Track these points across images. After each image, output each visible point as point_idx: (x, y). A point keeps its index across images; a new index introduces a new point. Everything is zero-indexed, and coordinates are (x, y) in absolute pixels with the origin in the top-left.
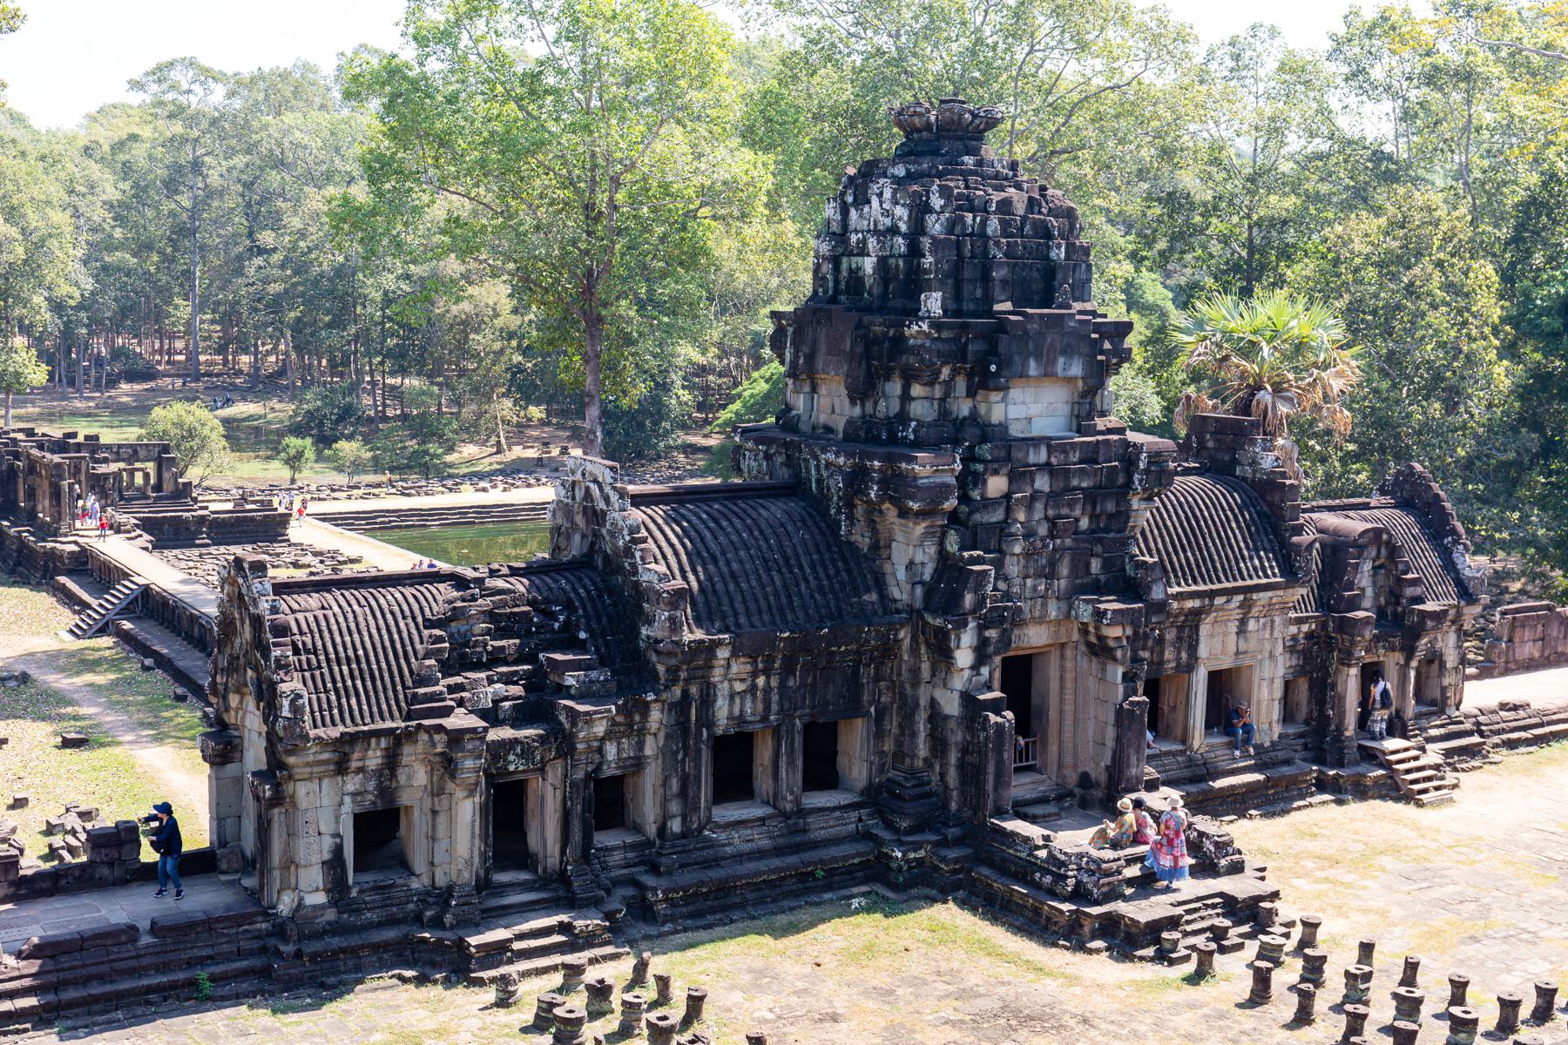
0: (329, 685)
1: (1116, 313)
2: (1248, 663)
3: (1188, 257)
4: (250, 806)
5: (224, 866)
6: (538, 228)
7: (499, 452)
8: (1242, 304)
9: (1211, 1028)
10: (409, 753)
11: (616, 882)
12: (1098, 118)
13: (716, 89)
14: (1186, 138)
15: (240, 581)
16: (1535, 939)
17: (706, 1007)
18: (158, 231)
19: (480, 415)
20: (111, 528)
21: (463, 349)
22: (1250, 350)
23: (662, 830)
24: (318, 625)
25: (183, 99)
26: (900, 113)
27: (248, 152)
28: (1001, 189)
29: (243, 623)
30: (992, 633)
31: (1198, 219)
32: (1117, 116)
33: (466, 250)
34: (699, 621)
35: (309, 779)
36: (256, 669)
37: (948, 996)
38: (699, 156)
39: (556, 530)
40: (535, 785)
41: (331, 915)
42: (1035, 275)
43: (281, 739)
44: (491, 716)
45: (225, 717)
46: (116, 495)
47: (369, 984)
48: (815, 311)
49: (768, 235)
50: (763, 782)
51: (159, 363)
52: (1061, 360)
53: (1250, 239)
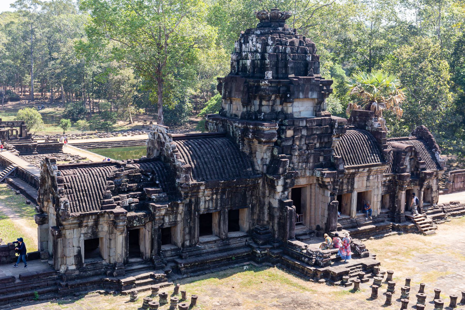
0: (76, 199)
1: (328, 77)
2: (370, 190)
3: (350, 60)
4: (51, 238)
5: (43, 257)
6: (142, 51)
7: (130, 123)
8: (368, 75)
9: (359, 307)
10: (102, 220)
11: (169, 261)
12: (321, 15)
13: (199, 6)
14: (350, 21)
15: (47, 165)
16: (461, 278)
17: (197, 301)
18: (20, 53)
19: (124, 111)
20: (5, 148)
21: (118, 90)
22: (370, 89)
23: (183, 245)
24: (73, 179)
25: (28, 10)
26: (258, 14)
27: (49, 27)
28: (291, 38)
29: (48, 179)
30: (288, 181)
31: (353, 47)
32: (328, 14)
33: (119, 58)
34: (195, 178)
35: (70, 229)
36: (53, 193)
37: (275, 297)
38: (194, 28)
39: (149, 148)
40: (142, 230)
41: (77, 273)
42: (302, 66)
43: (61, 216)
44: (128, 208)
45: (43, 209)
46: (7, 138)
47: (90, 295)
48: (232, 77)
49: (216, 53)
50: (215, 229)
51: (21, 95)
52: (310, 93)
53: (370, 54)
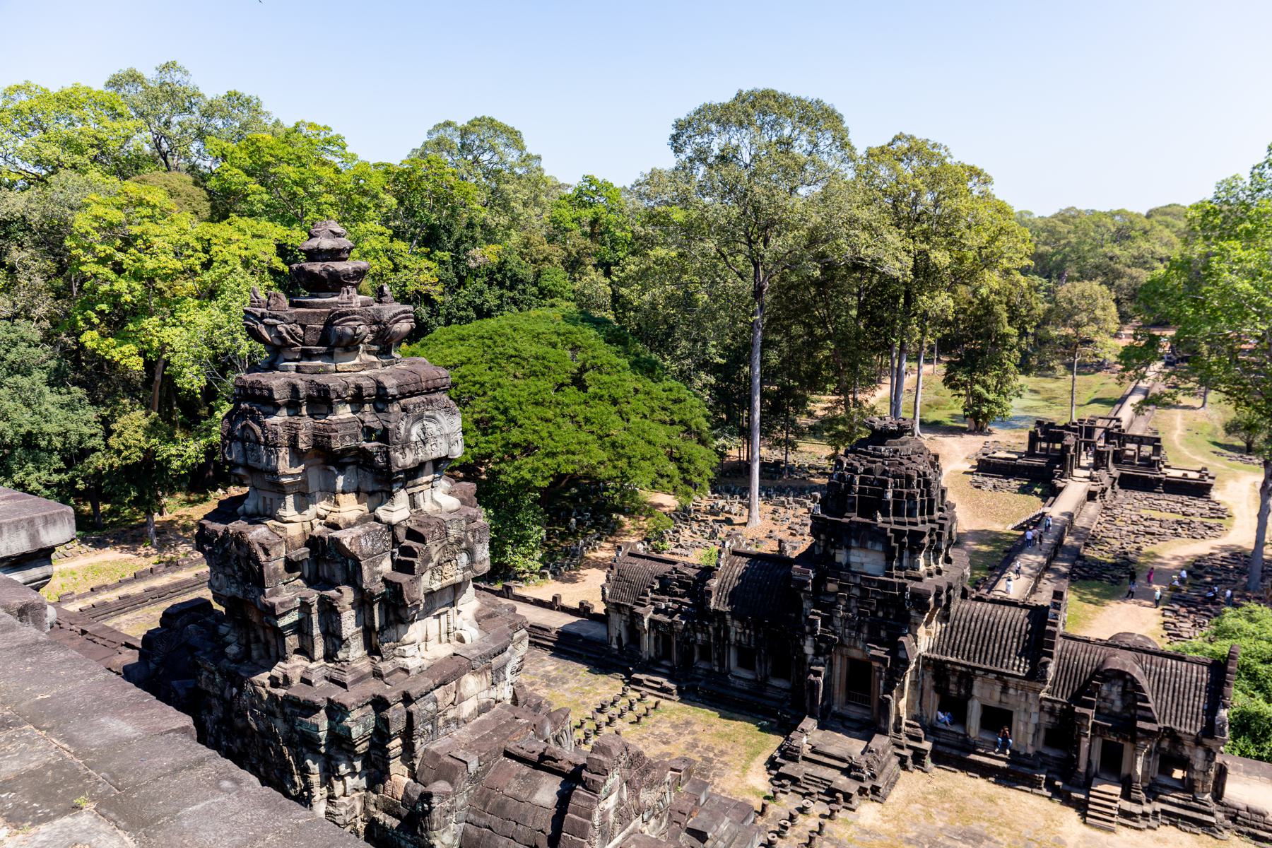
30: (823, 645)
52: (869, 543)
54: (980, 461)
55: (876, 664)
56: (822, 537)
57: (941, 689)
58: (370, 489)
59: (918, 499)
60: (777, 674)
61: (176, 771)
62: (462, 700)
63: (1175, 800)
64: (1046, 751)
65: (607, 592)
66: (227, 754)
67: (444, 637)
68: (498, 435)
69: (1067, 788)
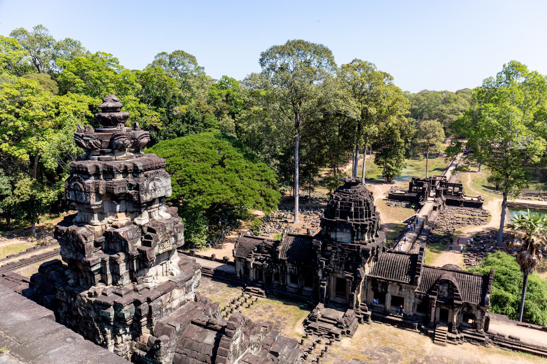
30: (326, 273)
52: (345, 230)
54: (390, 195)
55: (348, 280)
56: (325, 227)
57: (374, 289)
58: (131, 211)
59: (364, 211)
60: (307, 285)
61: (46, 334)
62: (173, 300)
63: (469, 332)
64: (418, 314)
65: (235, 252)
66: (69, 327)
67: (165, 273)
68: (187, 187)
69: (426, 328)
